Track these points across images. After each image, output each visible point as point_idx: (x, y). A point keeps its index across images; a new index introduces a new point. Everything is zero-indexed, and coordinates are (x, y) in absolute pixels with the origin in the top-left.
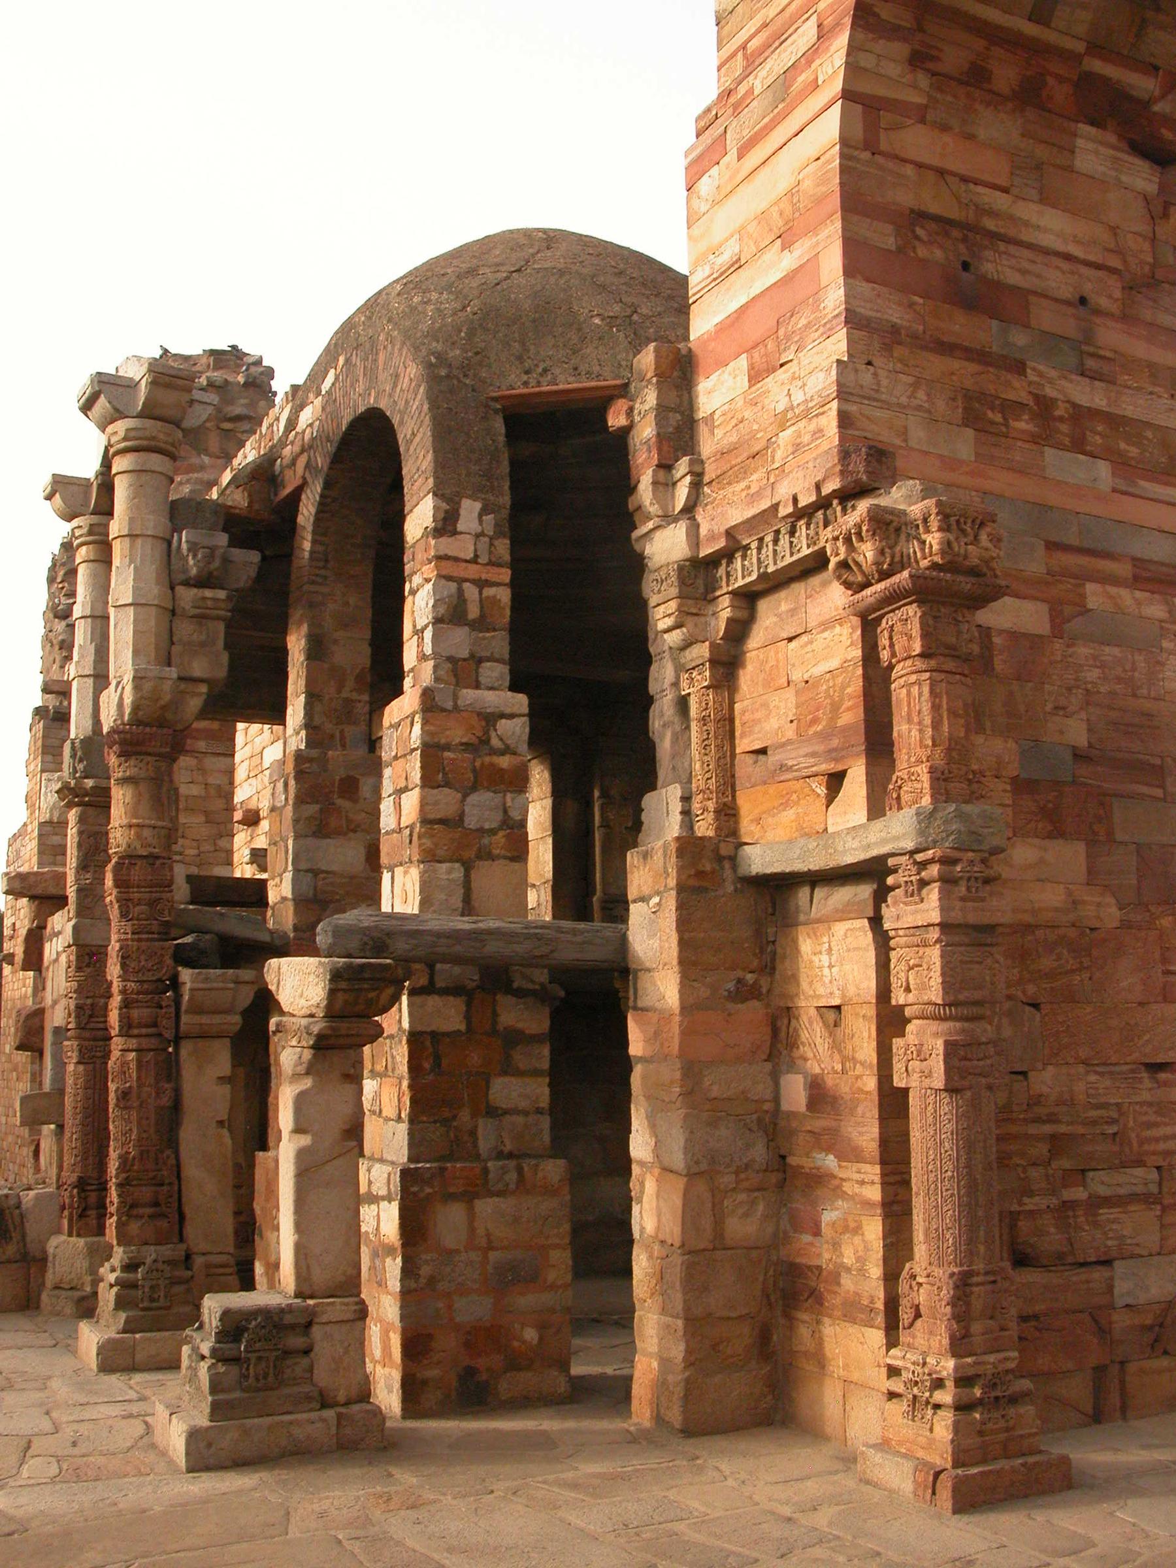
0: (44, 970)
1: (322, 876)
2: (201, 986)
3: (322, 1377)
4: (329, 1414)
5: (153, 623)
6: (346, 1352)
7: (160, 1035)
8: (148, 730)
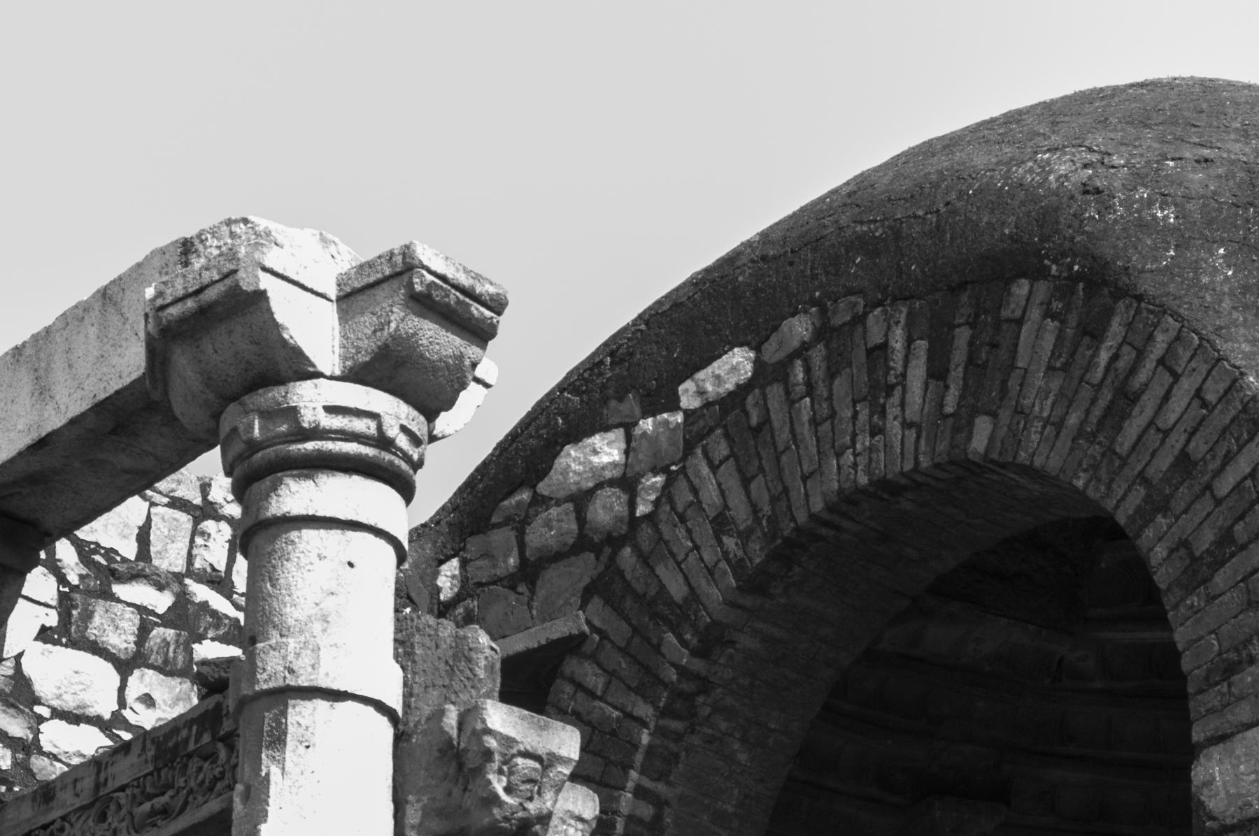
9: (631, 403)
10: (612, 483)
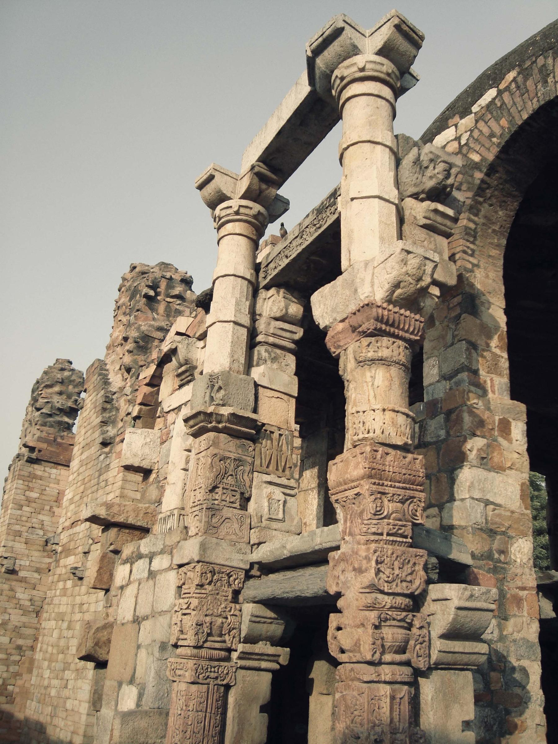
0: (113, 592)
1: (492, 507)
9: (457, 118)
10: (452, 141)
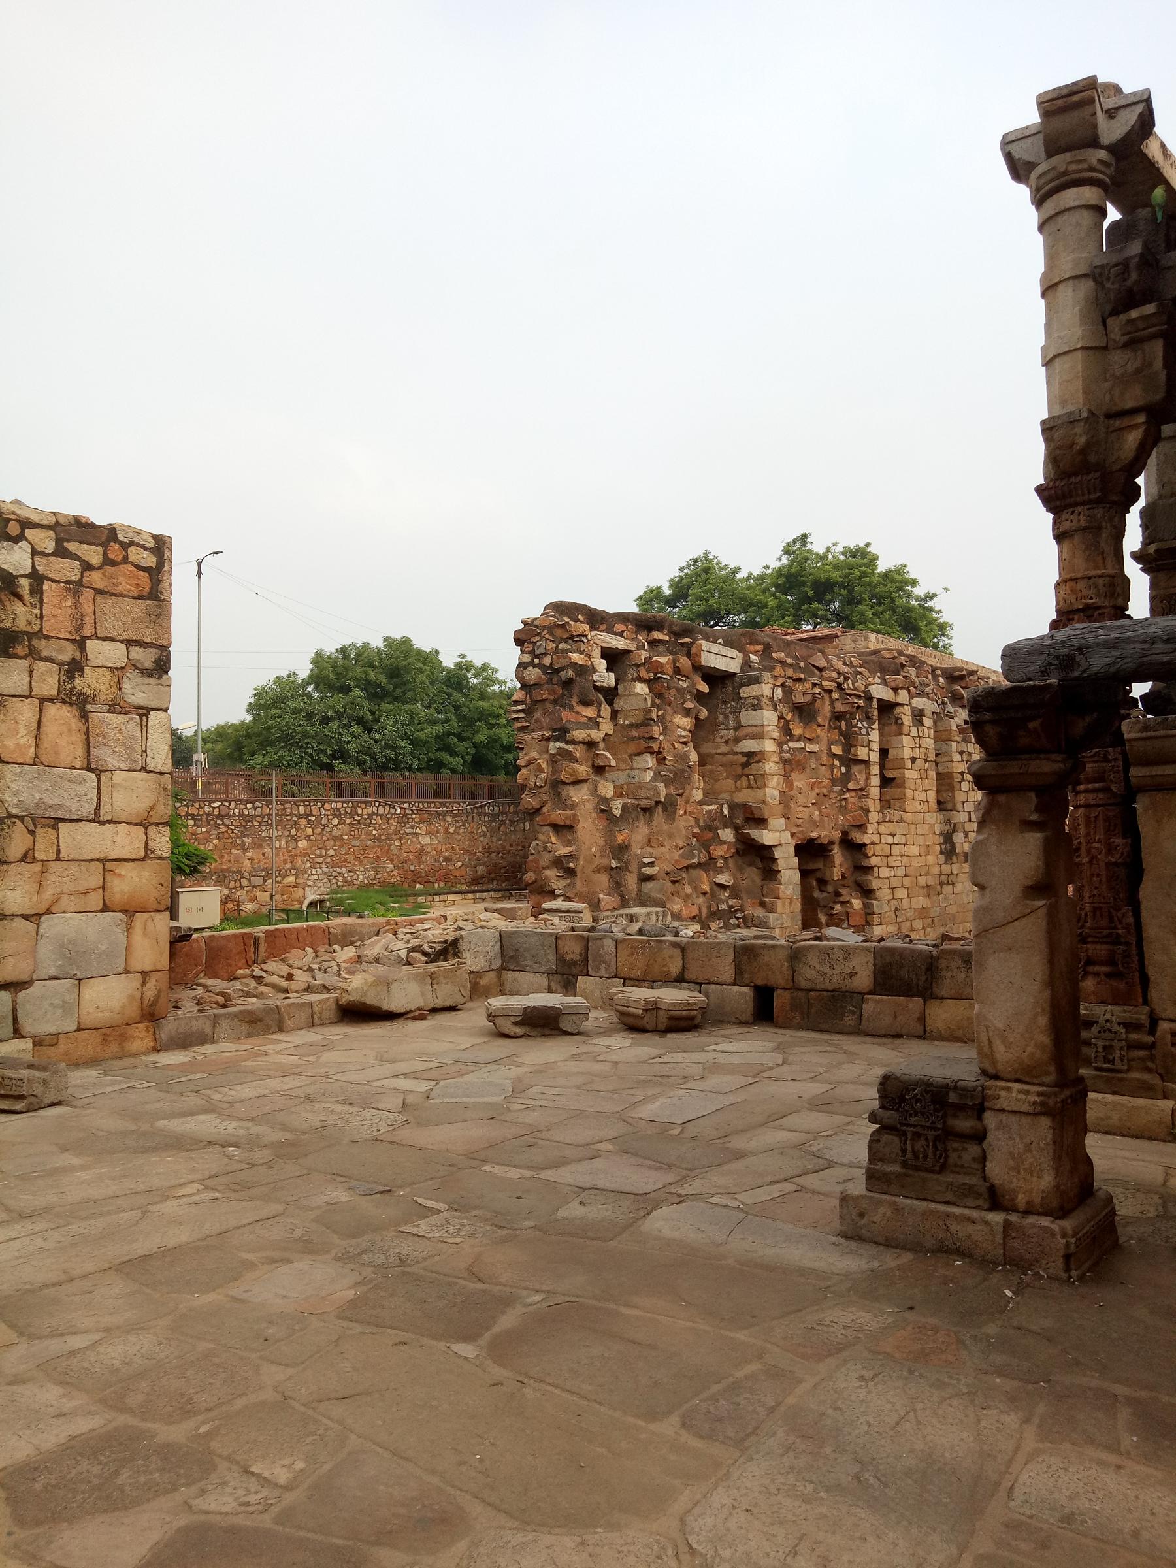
2: (1138, 735)
3: (997, 1170)
4: (997, 1218)
5: (1079, 367)
6: (1028, 1148)
7: (1106, 790)
8: (1073, 479)
